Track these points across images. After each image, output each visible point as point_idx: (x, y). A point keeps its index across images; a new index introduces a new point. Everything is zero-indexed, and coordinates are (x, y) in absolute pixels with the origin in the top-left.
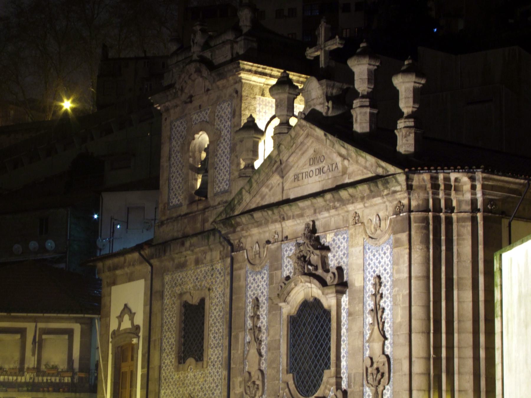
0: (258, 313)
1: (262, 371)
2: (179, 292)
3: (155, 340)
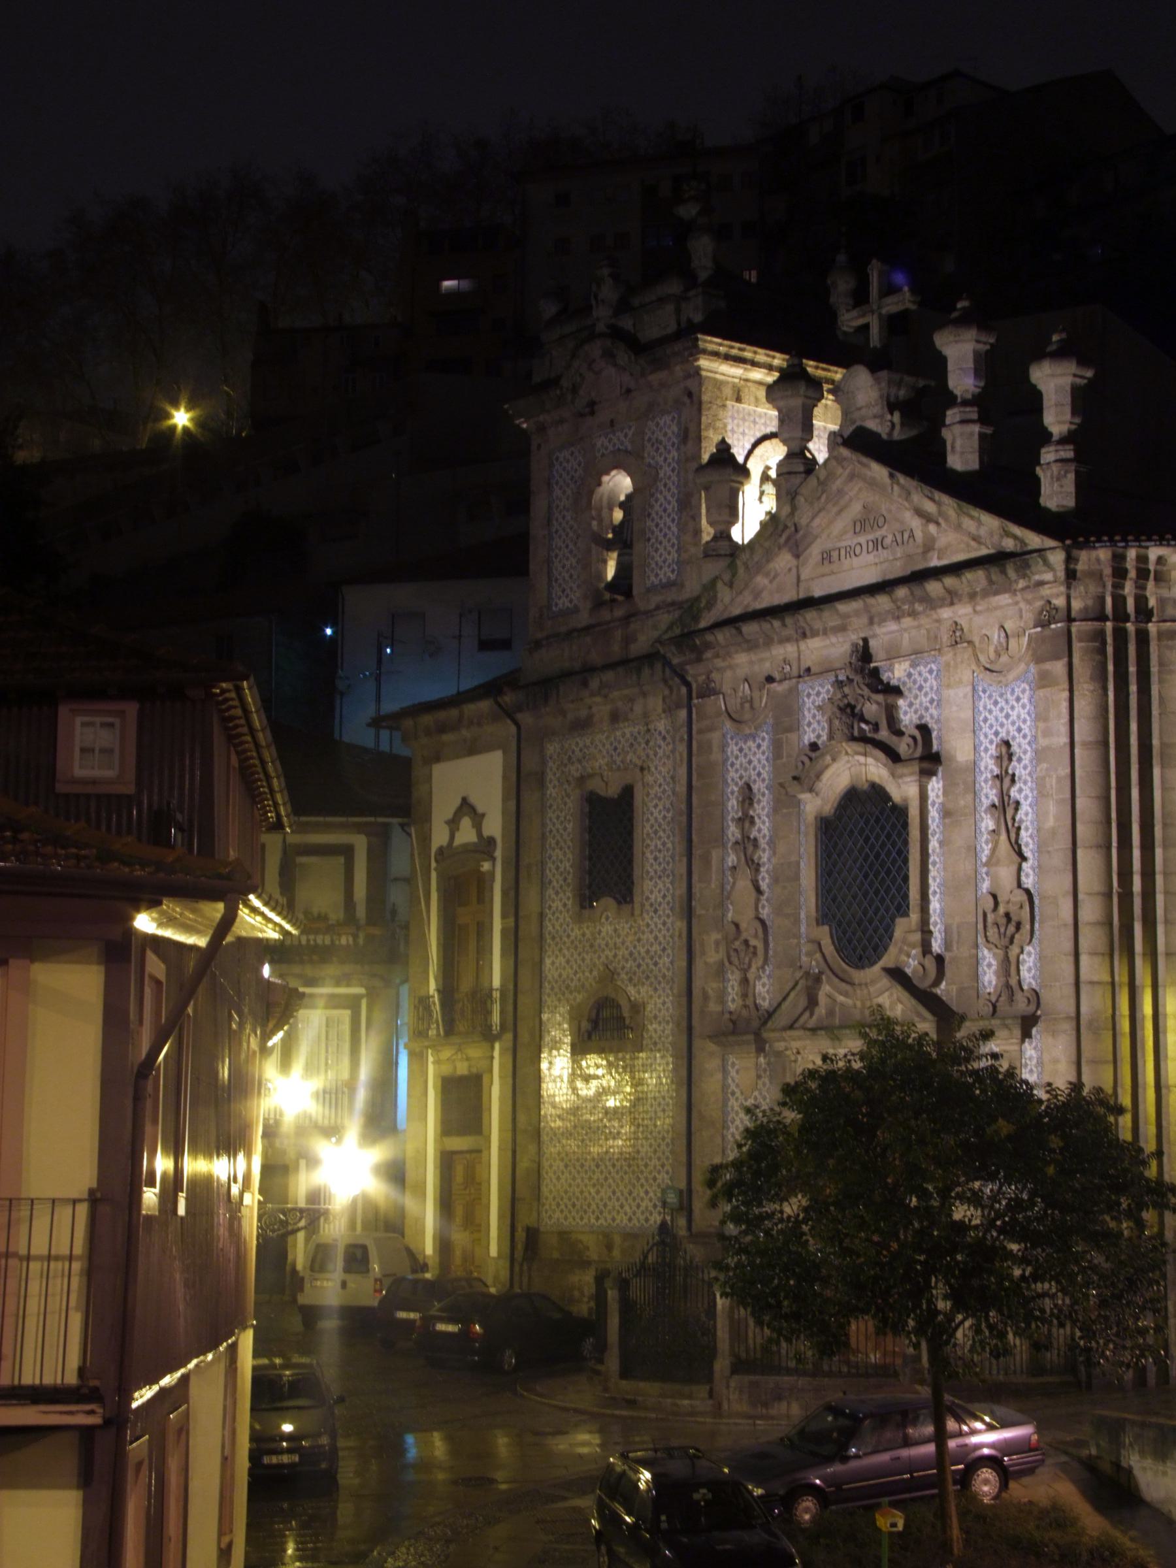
0: (751, 813)
1: (762, 922)
2: (577, 775)
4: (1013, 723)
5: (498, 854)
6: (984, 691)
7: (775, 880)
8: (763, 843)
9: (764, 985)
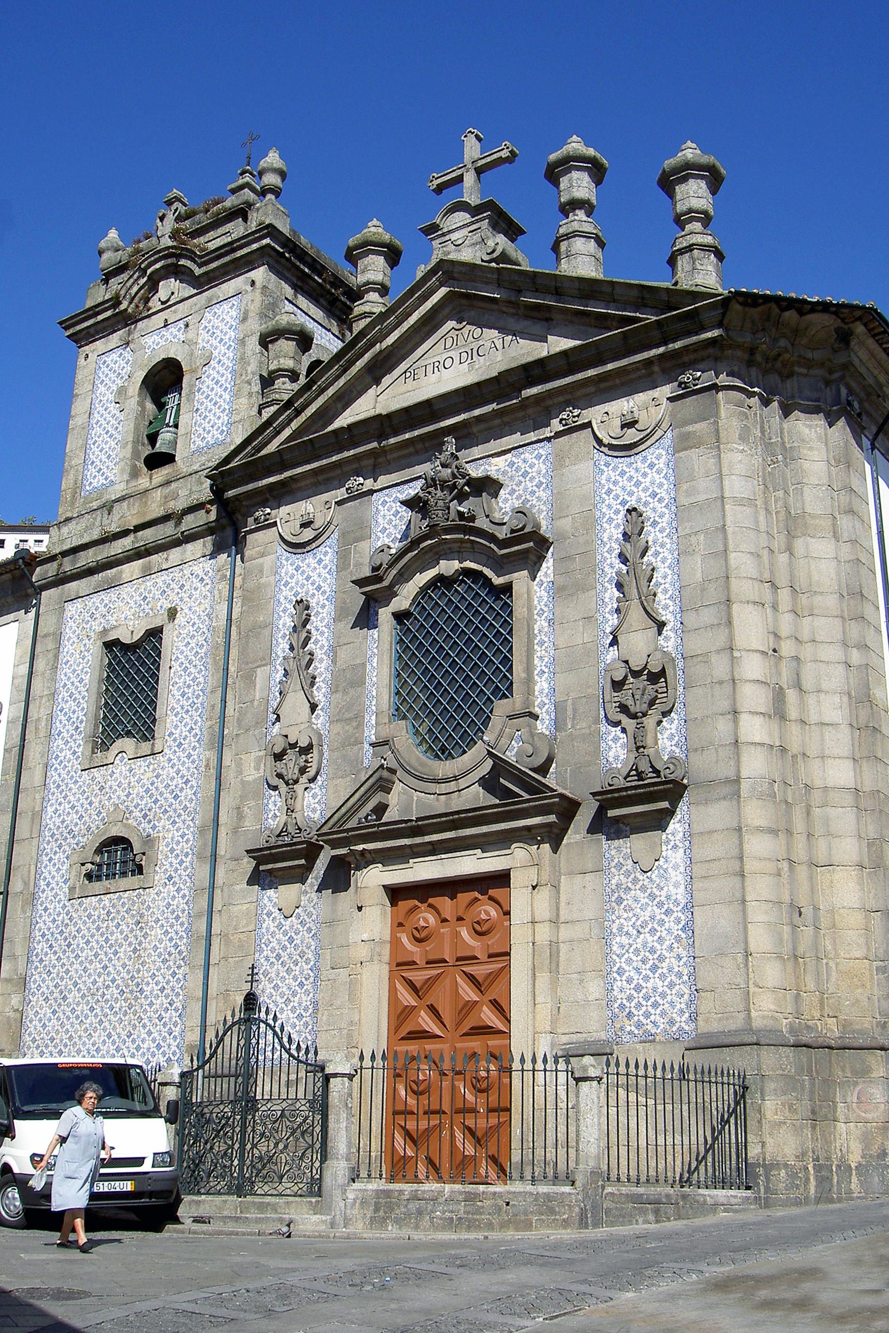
2: (101, 629)
3: (38, 719)
4: (645, 490)
6: (607, 465)
7: (334, 689)
8: (319, 654)
9: (314, 796)
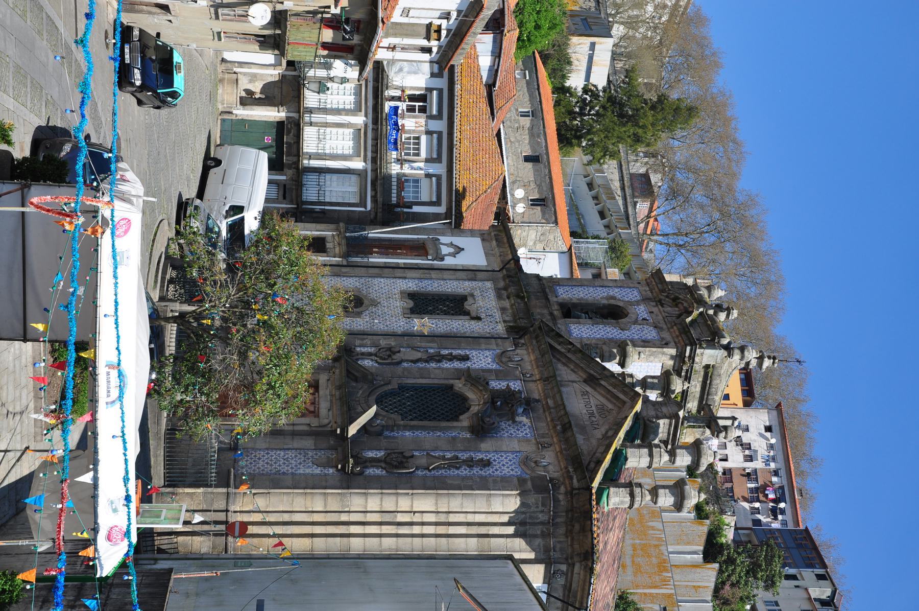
5: (435, 262)
